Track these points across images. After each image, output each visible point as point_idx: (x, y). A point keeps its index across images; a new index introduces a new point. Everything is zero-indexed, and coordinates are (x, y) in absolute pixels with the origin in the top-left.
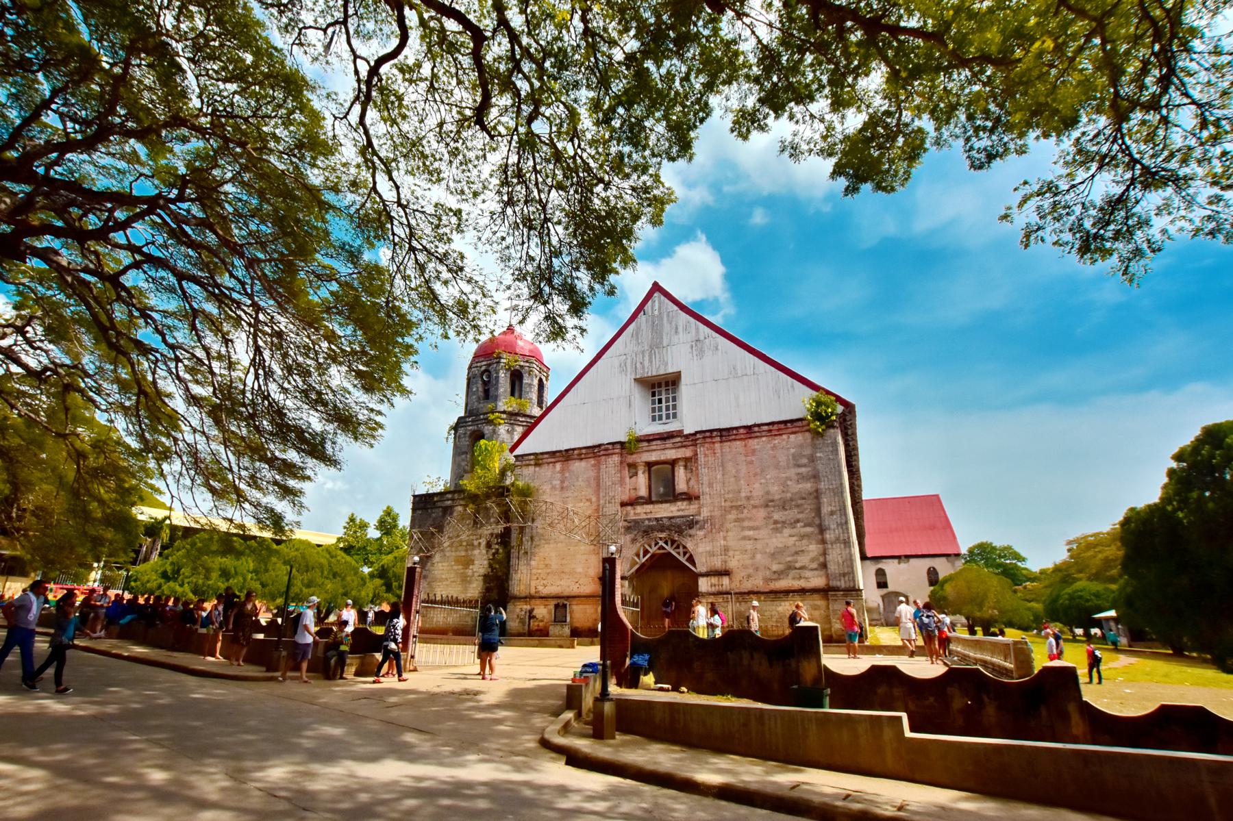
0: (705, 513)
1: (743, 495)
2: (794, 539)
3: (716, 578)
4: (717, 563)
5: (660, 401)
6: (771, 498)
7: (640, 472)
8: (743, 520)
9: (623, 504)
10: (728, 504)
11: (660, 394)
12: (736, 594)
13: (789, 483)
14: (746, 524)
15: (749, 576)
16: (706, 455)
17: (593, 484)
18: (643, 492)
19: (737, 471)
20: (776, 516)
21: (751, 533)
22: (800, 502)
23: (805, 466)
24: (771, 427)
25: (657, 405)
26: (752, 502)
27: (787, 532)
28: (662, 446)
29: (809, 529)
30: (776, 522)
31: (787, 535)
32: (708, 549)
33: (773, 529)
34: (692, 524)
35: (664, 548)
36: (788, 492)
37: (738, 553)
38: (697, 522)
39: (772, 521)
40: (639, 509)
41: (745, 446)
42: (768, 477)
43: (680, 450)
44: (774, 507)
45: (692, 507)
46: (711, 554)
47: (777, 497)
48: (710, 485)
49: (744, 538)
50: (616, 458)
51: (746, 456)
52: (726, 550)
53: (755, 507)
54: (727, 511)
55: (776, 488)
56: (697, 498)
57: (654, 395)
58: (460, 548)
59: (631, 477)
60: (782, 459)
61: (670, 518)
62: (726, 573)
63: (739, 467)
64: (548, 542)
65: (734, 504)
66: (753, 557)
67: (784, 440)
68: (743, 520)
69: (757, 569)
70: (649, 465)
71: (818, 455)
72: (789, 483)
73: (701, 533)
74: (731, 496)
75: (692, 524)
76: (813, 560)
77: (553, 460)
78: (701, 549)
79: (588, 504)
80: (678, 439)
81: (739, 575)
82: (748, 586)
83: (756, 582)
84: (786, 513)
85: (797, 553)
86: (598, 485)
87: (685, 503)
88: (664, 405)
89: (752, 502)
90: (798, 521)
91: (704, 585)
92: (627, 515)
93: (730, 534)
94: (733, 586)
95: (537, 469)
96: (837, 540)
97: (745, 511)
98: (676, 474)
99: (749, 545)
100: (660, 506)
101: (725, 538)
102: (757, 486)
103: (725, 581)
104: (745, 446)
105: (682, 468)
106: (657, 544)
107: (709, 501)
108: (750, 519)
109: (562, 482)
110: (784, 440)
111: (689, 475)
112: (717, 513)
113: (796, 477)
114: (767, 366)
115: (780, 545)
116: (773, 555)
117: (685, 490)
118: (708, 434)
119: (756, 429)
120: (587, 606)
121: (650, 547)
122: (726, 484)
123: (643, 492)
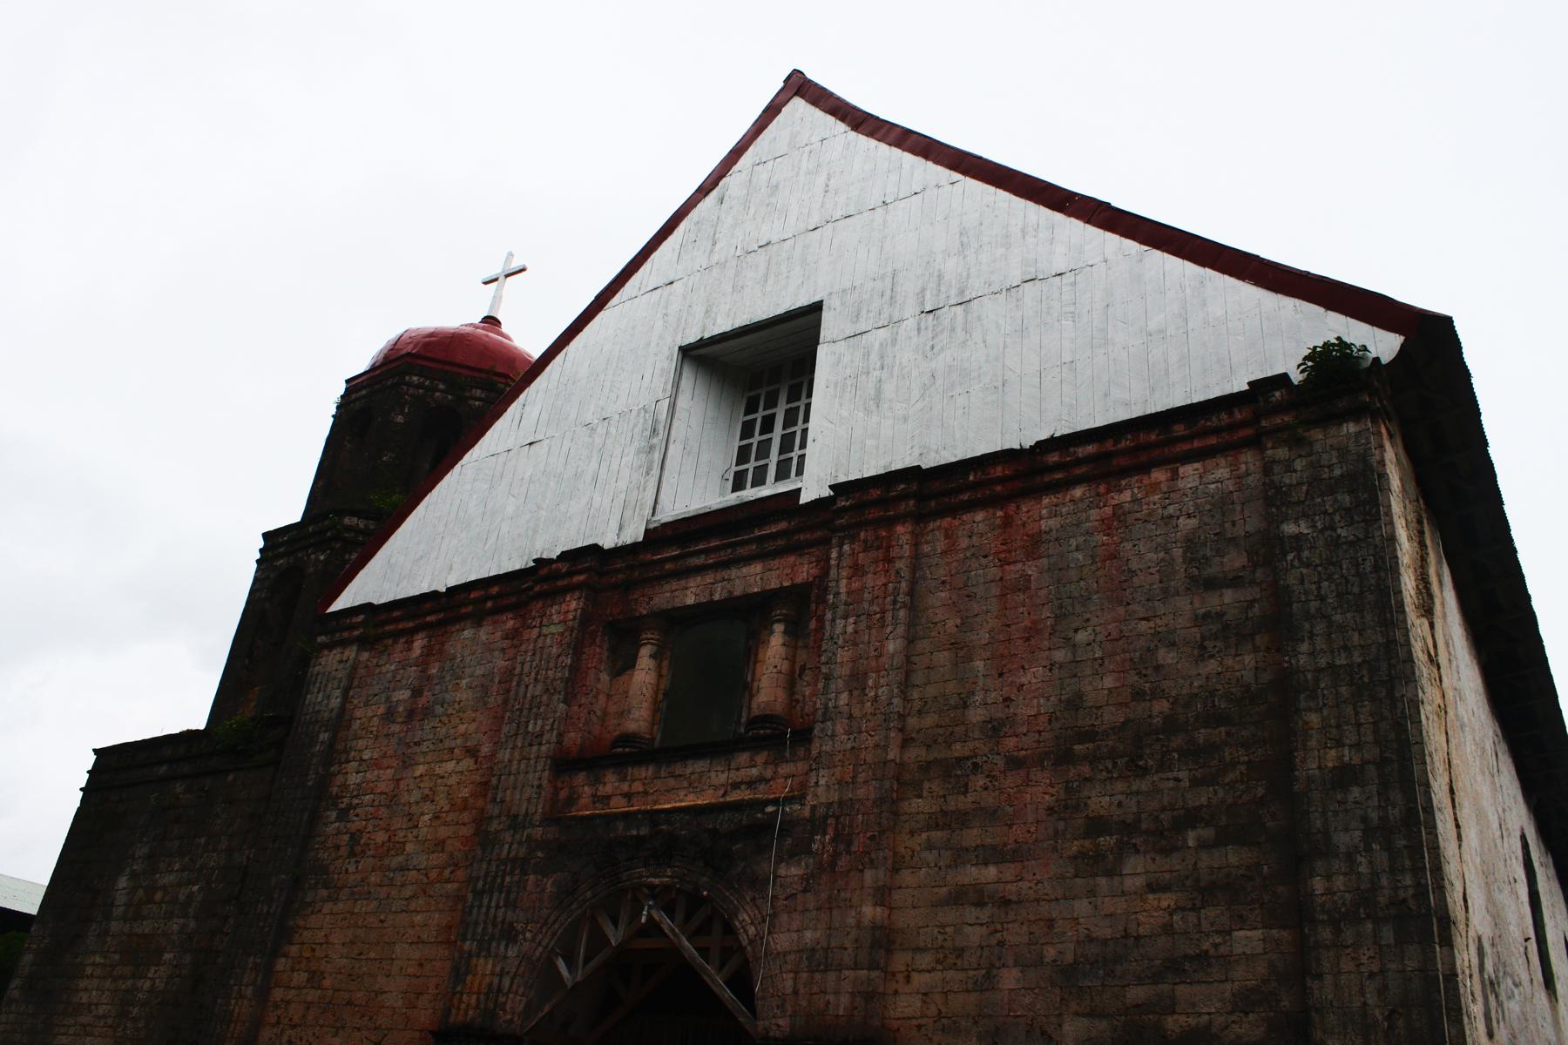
0: (823, 788)
1: (976, 715)
2: (1167, 900)
5: (768, 425)
8: (962, 819)
10: (915, 753)
11: (772, 403)
13: (1166, 656)
16: (857, 570)
17: (494, 700)
18: (638, 718)
19: (965, 625)
20: (1100, 801)
22: (1202, 735)
23: (1235, 582)
24: (1109, 445)
26: (1011, 743)
27: (1136, 869)
28: (724, 555)
29: (1234, 857)
30: (1096, 826)
31: (1139, 882)
33: (1082, 855)
36: (1157, 694)
37: (925, 960)
40: (611, 783)
41: (1007, 523)
42: (1082, 637)
43: (775, 563)
44: (1093, 759)
45: (785, 769)
46: (818, 960)
47: (1111, 716)
48: (857, 681)
49: (958, 897)
50: (573, 604)
51: (1005, 563)
53: (1014, 763)
55: (1109, 682)
57: (751, 408)
60: (1142, 554)
63: (975, 607)
65: (936, 754)
66: (987, 982)
67: (1155, 487)
68: (962, 819)
71: (1290, 528)
72: (1166, 656)
74: (930, 720)
76: (1244, 1002)
77: (411, 624)
78: (782, 941)
79: (468, 763)
80: (783, 525)
84: (1143, 785)
85: (1174, 967)
89: (1011, 743)
90: (1191, 818)
92: (572, 800)
93: (906, 877)
95: (365, 655)
97: (981, 781)
99: (973, 928)
104: (1007, 523)
105: (779, 628)
107: (843, 742)
108: (992, 814)
109: (417, 693)
110: (1155, 487)
113: (1195, 633)
114: (1112, 240)
115: (1104, 931)
116: (1068, 975)
117: (779, 709)
118: (875, 493)
119: (1054, 458)
122: (918, 679)
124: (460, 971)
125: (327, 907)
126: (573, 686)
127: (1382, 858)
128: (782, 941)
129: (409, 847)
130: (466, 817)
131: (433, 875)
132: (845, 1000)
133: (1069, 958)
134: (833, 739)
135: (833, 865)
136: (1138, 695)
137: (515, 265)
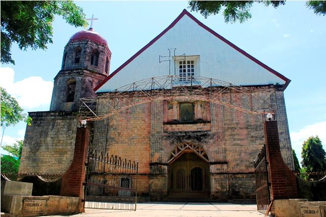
0: (214, 130)
1: (234, 122)
3: (220, 165)
4: (220, 157)
6: (250, 124)
7: (175, 107)
8: (234, 135)
9: (165, 123)
10: (226, 126)
12: (231, 173)
13: (259, 117)
14: (236, 137)
15: (238, 165)
20: (252, 134)
21: (239, 142)
25: (183, 73)
26: (239, 126)
27: (258, 142)
30: (252, 137)
32: (215, 149)
34: (205, 136)
35: (189, 149)
36: (258, 121)
38: (209, 135)
39: (250, 136)
40: (174, 126)
44: (251, 129)
45: (206, 127)
46: (217, 152)
47: (252, 124)
48: (217, 115)
49: (235, 145)
52: (225, 150)
53: (241, 128)
54: (225, 130)
55: (252, 119)
56: (209, 122)
58: (58, 144)
59: (169, 109)
61: (194, 132)
62: (226, 163)
64: (117, 142)
65: (230, 126)
66: (240, 155)
68: (234, 135)
69: (242, 161)
70: (180, 103)
72: (259, 117)
73: (211, 141)
74: (228, 122)
75: (205, 136)
78: (211, 150)
79: (143, 122)
81: (232, 165)
82: (237, 170)
83: (241, 168)
84: (258, 132)
86: (150, 112)
87: (202, 124)
88: (187, 73)
91: (213, 169)
94: (229, 170)
96: (284, 146)
97: (236, 130)
98: (196, 109)
99: (238, 148)
100: (187, 125)
101: (225, 144)
102: (242, 117)
103: (225, 167)
106: (185, 146)
111: (203, 110)
112: (220, 131)
115: (254, 149)
116: (250, 154)
117: (201, 118)
120: (142, 180)
121: (182, 147)
123: (176, 117)
124: (152, 155)
125: (116, 145)
126: (164, 111)
127: (286, 142)
128: (211, 150)
129: (133, 135)
130: (145, 131)
131: (140, 140)
132: (222, 158)
133: (250, 152)
134: (214, 123)
135: (217, 140)
136: (256, 121)
137: (94, 17)
